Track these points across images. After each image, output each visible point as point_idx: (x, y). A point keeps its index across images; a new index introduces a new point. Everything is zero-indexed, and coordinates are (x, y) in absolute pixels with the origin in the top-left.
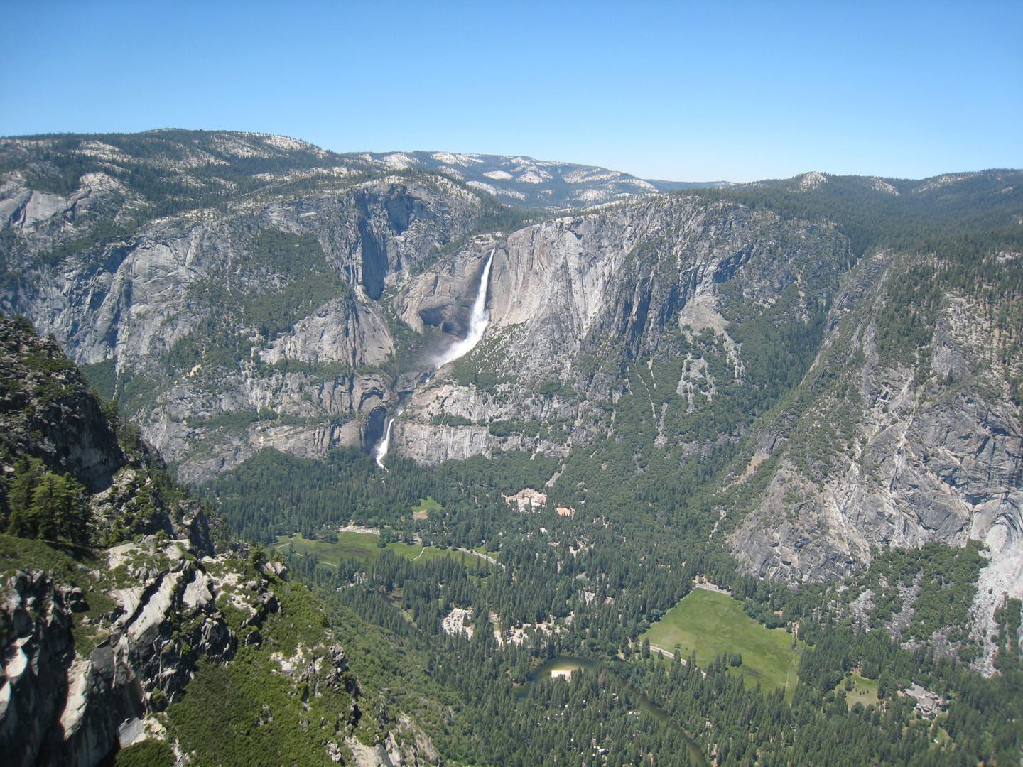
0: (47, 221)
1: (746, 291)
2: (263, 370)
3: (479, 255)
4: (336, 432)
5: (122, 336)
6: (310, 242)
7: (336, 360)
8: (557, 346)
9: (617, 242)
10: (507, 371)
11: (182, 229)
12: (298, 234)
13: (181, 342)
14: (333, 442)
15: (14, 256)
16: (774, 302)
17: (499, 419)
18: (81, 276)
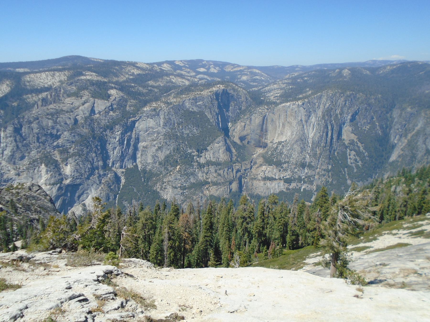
1: (359, 124)
2: (201, 166)
3: (261, 115)
4: (231, 186)
5: (139, 155)
6: (202, 114)
7: (225, 160)
8: (303, 150)
9: (314, 109)
10: (285, 159)
11: (156, 112)
12: (197, 111)
13: (167, 157)
14: (231, 190)
16: (369, 128)
17: (286, 177)
18: (122, 134)
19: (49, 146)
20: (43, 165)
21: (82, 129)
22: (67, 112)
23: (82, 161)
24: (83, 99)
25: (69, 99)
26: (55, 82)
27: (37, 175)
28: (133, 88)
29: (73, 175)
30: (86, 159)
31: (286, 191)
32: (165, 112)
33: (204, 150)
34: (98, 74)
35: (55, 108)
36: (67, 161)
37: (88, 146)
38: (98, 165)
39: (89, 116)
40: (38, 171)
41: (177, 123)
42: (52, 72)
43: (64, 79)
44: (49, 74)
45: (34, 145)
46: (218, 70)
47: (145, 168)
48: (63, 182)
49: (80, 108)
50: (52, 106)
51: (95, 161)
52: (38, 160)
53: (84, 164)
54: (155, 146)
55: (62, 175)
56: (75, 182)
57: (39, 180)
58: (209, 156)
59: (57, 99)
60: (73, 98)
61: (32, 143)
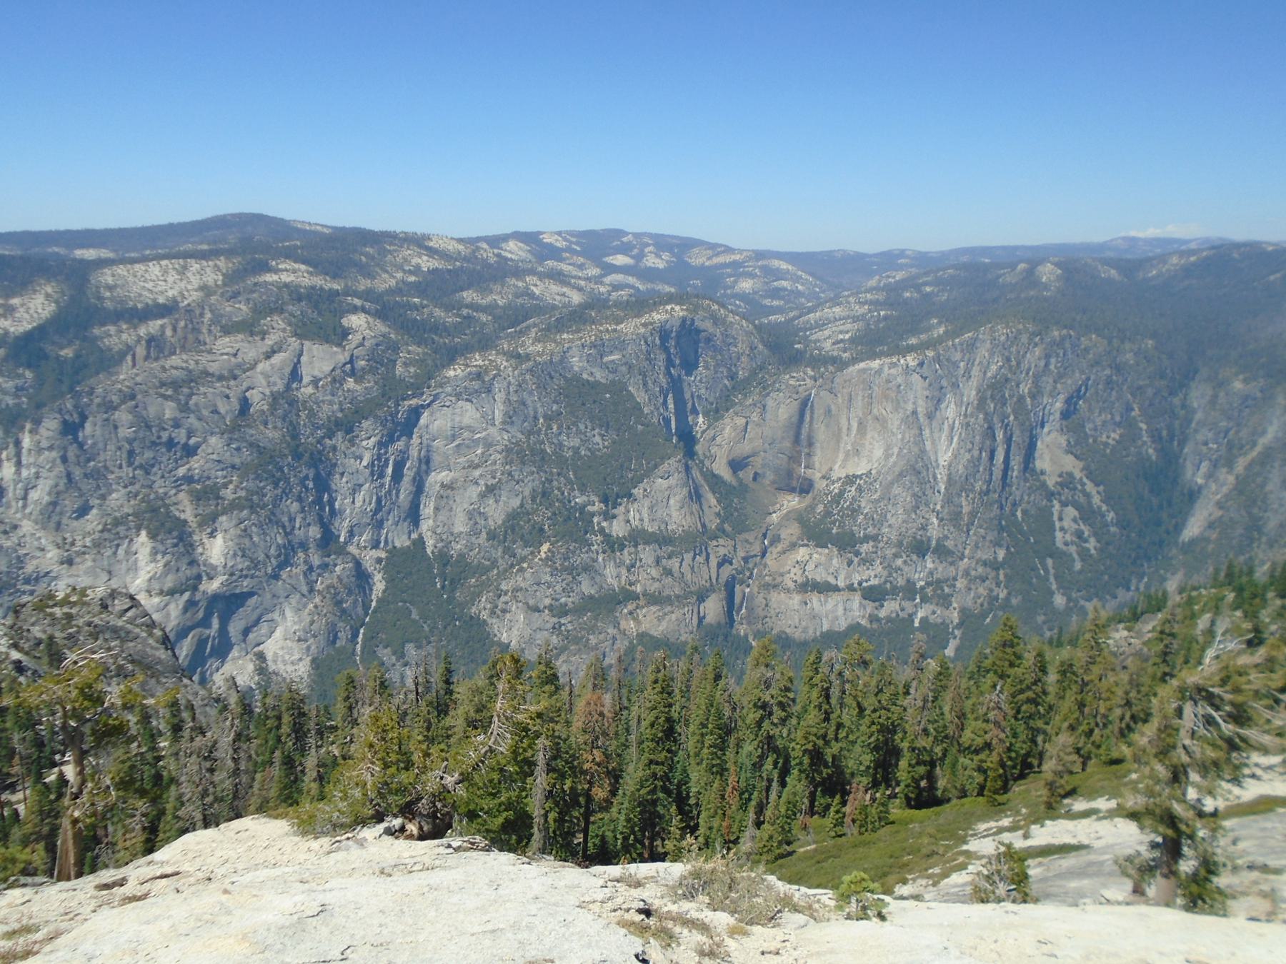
0: (326, 377)
1: (1089, 426)
2: (613, 545)
3: (796, 396)
4: (702, 608)
5: (427, 510)
6: (618, 388)
7: (686, 528)
8: (919, 501)
9: (954, 380)
10: (865, 529)
11: (483, 382)
12: (603, 381)
13: (513, 517)
14: (701, 620)
15: (305, 424)
16: (1117, 437)
17: (869, 583)
18: (380, 444)
19: (163, 477)
20: (144, 533)
21: (262, 428)
22: (221, 378)
23: (260, 526)
24: (270, 341)
25: (228, 339)
26: (188, 291)
27: (125, 563)
28: (418, 310)
29: (232, 567)
30: (270, 520)
31: (869, 626)
32: (509, 383)
33: (622, 497)
34: (315, 267)
35: (184, 365)
36: (214, 522)
37: (279, 480)
38: (307, 538)
39: (284, 392)
40: (127, 552)
41: (545, 417)
42: (181, 261)
43: (216, 281)
44: (171, 266)
45: (118, 473)
46: (667, 262)
47: (446, 550)
48: (202, 588)
49: (260, 367)
50: (175, 360)
51: (297, 525)
52: (130, 518)
53: (265, 534)
54: (476, 483)
55: (199, 565)
56: (236, 586)
57: (128, 579)
58: (637, 517)
59: (192, 340)
60: (240, 337)
61: (112, 468)
